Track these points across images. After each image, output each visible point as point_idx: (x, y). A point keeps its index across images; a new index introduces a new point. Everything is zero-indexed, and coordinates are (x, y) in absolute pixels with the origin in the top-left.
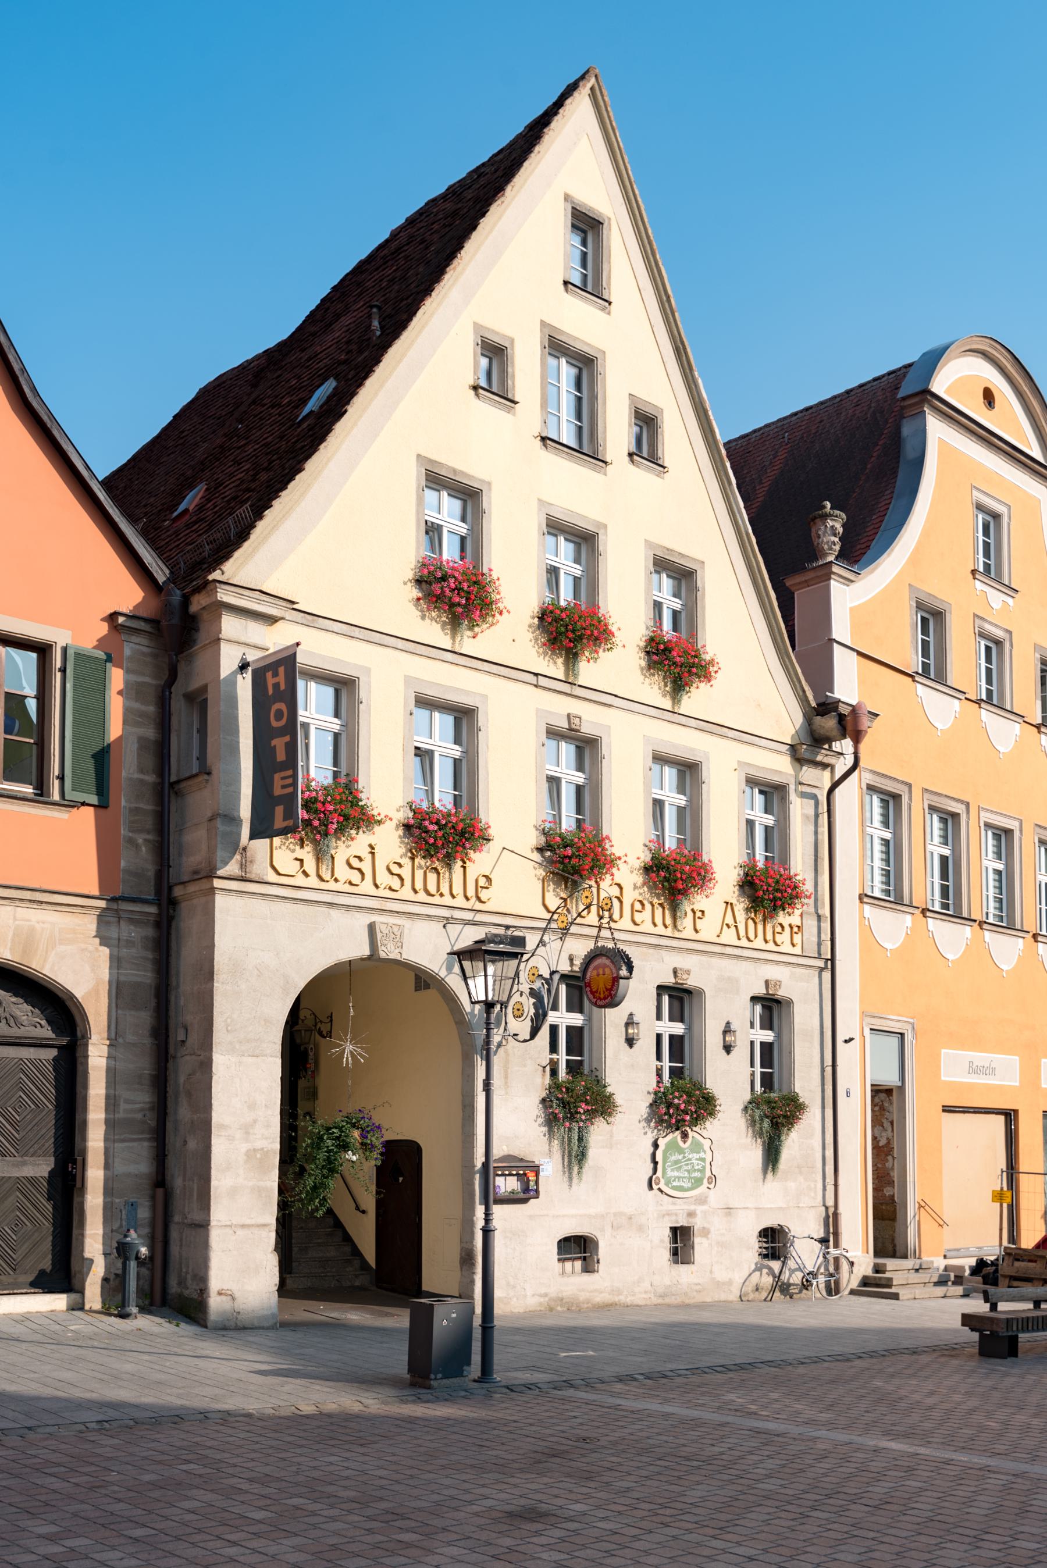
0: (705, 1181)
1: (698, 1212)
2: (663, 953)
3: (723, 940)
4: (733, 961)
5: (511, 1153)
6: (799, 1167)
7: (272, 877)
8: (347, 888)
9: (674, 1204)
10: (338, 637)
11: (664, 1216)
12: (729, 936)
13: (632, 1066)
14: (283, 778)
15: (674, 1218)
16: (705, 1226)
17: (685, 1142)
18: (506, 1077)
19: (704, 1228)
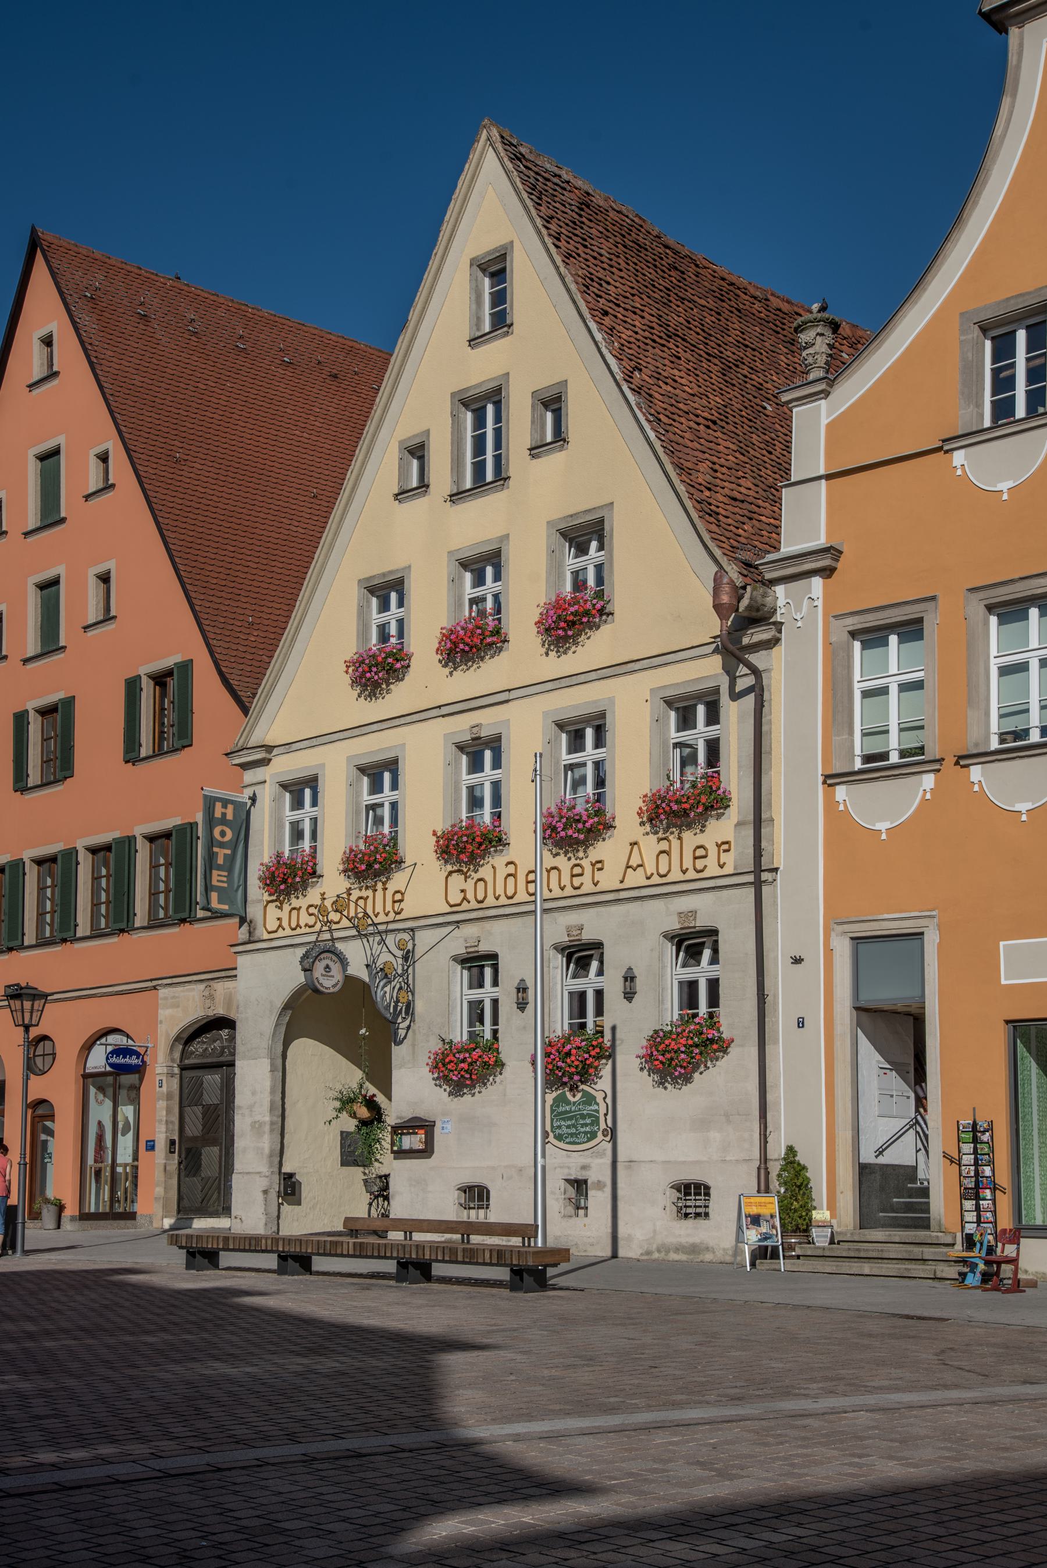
0: (600, 1134)
1: (592, 1165)
2: (556, 914)
3: (627, 884)
4: (638, 903)
5: (418, 1116)
6: (727, 1115)
7: (266, 936)
8: (308, 930)
9: (568, 1157)
10: (306, 751)
11: (555, 1168)
12: (635, 879)
13: (524, 1028)
14: (219, 875)
15: (566, 1171)
16: (601, 1179)
17: (574, 1096)
18: (414, 1053)
19: (599, 1181)
